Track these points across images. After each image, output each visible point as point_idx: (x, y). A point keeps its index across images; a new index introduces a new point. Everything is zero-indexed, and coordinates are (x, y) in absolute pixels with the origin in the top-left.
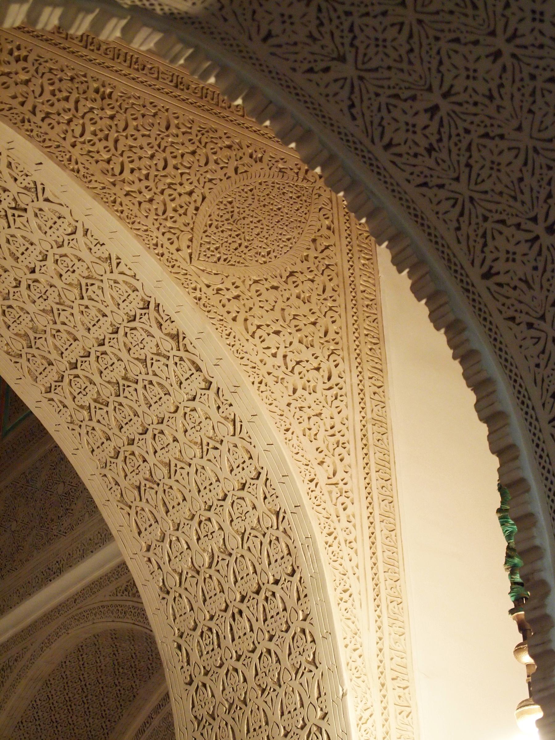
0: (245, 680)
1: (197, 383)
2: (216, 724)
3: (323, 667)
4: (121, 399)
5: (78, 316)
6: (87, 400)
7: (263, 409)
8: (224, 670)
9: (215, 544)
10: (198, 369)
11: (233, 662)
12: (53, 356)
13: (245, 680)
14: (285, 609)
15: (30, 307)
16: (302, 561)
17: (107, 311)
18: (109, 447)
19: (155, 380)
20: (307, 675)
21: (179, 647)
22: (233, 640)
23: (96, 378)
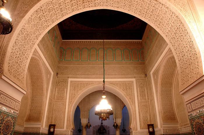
1: (161, 4)
3: (189, 33)
4: (153, 13)
5: (144, 5)
6: (149, 16)
7: (170, 4)
9: (170, 26)
10: (161, 3)
12: (144, 12)
15: (139, 7)
16: (182, 21)
17: (147, 2)
18: (154, 21)
19: (156, 8)
20: (187, 35)
23: (149, 12)
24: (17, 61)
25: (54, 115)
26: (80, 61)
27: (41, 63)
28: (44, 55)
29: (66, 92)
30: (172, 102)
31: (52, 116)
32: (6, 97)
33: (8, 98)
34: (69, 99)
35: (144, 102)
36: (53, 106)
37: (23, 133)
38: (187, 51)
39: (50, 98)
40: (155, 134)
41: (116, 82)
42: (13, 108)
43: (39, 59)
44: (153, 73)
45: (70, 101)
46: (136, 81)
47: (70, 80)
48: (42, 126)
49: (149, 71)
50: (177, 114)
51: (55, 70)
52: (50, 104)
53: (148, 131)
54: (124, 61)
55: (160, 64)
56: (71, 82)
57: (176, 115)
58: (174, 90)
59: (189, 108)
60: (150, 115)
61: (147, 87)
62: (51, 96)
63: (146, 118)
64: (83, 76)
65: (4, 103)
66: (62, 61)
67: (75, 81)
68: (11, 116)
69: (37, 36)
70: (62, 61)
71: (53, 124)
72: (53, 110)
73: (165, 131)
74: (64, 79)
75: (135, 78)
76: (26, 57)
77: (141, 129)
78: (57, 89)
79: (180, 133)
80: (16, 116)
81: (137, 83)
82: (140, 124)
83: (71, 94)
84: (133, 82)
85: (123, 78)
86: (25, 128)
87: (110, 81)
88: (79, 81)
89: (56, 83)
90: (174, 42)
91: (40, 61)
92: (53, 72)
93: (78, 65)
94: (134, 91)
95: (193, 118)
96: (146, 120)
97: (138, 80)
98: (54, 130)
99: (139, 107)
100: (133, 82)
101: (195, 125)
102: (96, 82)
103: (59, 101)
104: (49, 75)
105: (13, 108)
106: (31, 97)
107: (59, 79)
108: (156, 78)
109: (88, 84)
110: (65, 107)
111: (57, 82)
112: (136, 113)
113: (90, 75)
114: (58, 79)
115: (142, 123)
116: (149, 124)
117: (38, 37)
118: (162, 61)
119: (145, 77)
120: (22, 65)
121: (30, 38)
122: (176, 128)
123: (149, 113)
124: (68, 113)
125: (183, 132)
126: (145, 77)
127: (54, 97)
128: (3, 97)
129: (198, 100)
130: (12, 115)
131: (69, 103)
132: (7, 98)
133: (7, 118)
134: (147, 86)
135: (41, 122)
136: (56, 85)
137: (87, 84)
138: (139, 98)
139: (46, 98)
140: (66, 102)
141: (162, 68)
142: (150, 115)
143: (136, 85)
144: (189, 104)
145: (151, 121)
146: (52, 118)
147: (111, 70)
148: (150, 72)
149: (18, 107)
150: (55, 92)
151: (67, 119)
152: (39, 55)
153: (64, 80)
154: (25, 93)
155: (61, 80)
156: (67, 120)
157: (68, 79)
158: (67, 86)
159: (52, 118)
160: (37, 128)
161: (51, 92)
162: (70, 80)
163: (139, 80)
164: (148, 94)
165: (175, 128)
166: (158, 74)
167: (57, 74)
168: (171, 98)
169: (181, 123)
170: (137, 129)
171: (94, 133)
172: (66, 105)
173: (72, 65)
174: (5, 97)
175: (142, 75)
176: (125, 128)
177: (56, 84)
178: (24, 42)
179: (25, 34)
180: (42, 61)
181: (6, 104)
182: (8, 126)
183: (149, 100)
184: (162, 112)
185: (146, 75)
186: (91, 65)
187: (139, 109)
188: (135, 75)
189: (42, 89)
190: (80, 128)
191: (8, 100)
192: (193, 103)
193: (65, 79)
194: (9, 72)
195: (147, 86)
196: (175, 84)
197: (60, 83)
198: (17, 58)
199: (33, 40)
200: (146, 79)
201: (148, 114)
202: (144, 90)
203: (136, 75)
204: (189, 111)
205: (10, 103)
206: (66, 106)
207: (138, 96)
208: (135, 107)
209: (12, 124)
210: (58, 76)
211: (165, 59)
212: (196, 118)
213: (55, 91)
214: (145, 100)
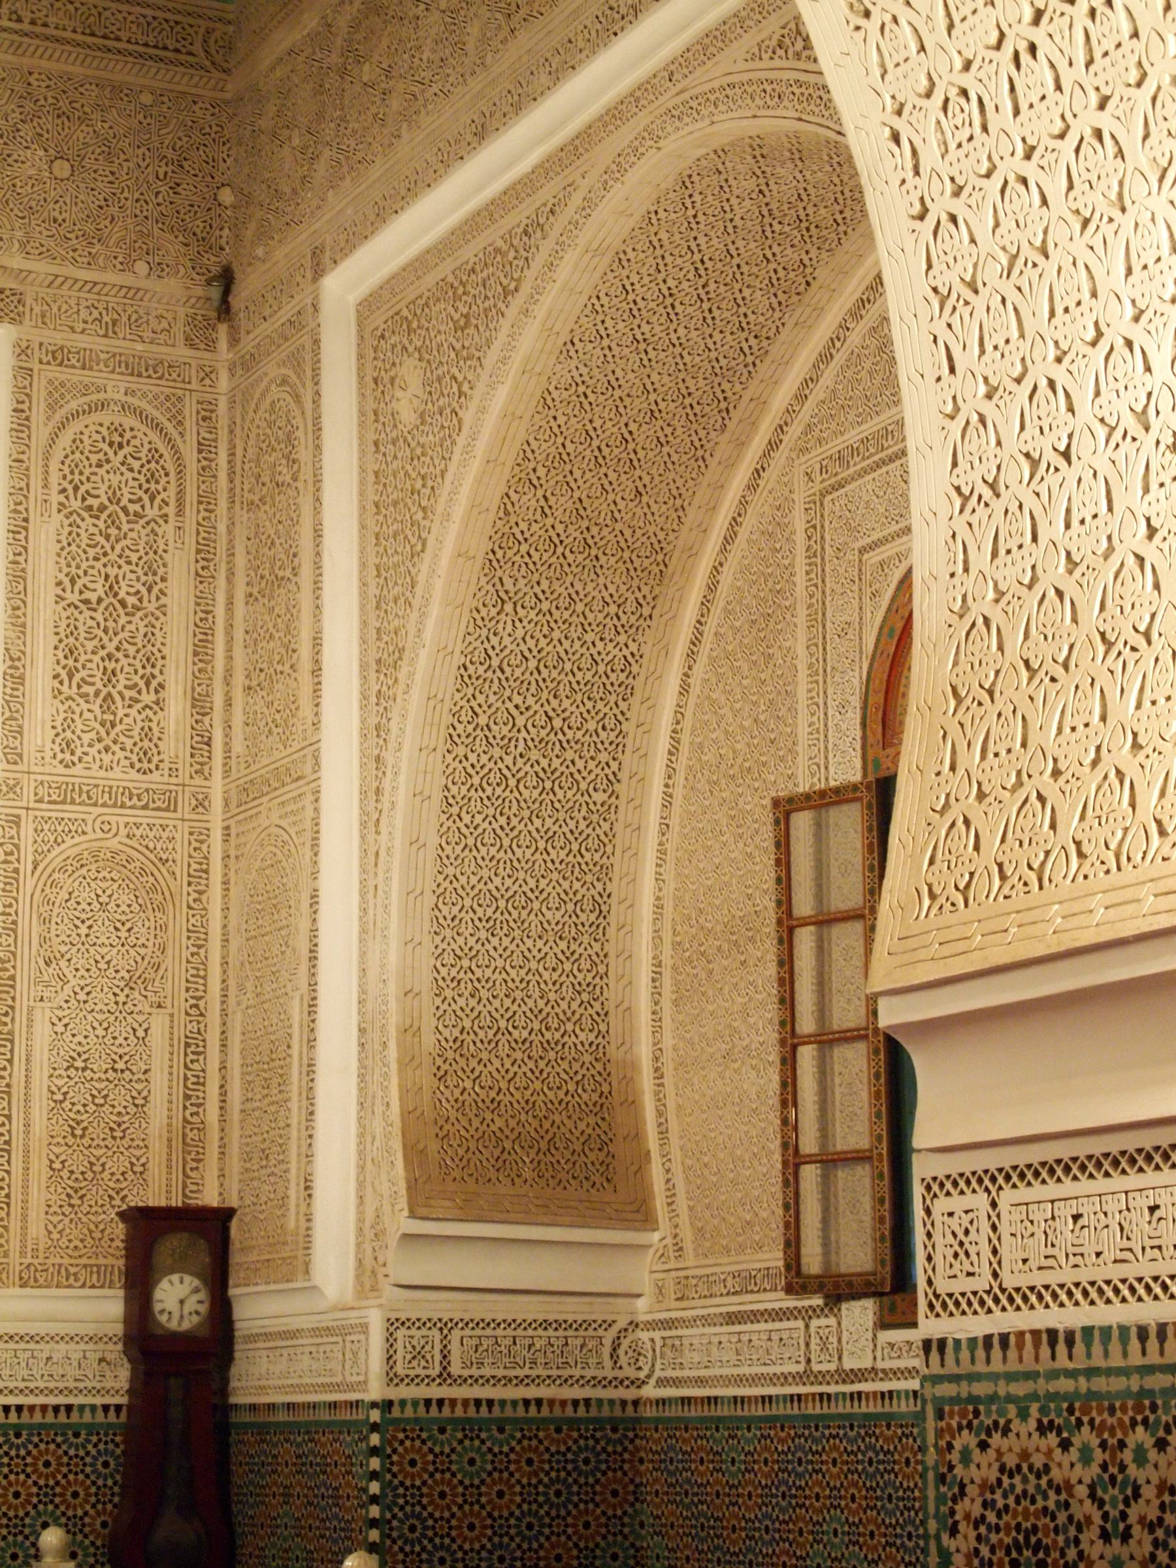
0: (1044, 202)
2: (978, 302)
8: (997, 181)
11: (1017, 165)
13: (1044, 202)
14: (1135, 35)
21: (896, 138)
22: (1017, 112)
30: (605, 872)
35: (119, 799)
38: (1120, 408)
40: (234, 1371)
44: (367, 307)
49: (298, 243)
50: (646, 1081)
53: (119, 1329)
55: (546, 194)
57: (633, 1104)
58: (684, 689)
59: (961, 1251)
60: (193, 1046)
61: (206, 531)
63: (120, 1098)
73: (418, 1355)
79: (650, 1391)
81: (40, 432)
90: (969, 167)
95: (973, 1399)
96: (117, 1131)
97: (59, 356)
101: (985, 1486)
108: (408, 416)
116: (157, 1198)
118: (603, 154)
122: (598, 1310)
123: (181, 1002)
125: (701, 1381)
129: (1101, 1184)
134: (206, 501)
141: (563, 272)
142: (193, 1046)
144: (969, 1201)
148: (318, 273)
163: (76, 376)
164: (201, 651)
165: (572, 1310)
166: (471, 357)
168: (609, 808)
169: (687, 1234)
175: (158, 269)
184: (429, 1023)
185: (227, 279)
188: (16, 262)
192: (1024, 1193)
195: (206, 501)
196: (726, 579)
200: (208, 374)
201: (159, 1025)
203: (42, 267)
204: (943, 1286)
211: (652, 136)
212: (1024, 1415)
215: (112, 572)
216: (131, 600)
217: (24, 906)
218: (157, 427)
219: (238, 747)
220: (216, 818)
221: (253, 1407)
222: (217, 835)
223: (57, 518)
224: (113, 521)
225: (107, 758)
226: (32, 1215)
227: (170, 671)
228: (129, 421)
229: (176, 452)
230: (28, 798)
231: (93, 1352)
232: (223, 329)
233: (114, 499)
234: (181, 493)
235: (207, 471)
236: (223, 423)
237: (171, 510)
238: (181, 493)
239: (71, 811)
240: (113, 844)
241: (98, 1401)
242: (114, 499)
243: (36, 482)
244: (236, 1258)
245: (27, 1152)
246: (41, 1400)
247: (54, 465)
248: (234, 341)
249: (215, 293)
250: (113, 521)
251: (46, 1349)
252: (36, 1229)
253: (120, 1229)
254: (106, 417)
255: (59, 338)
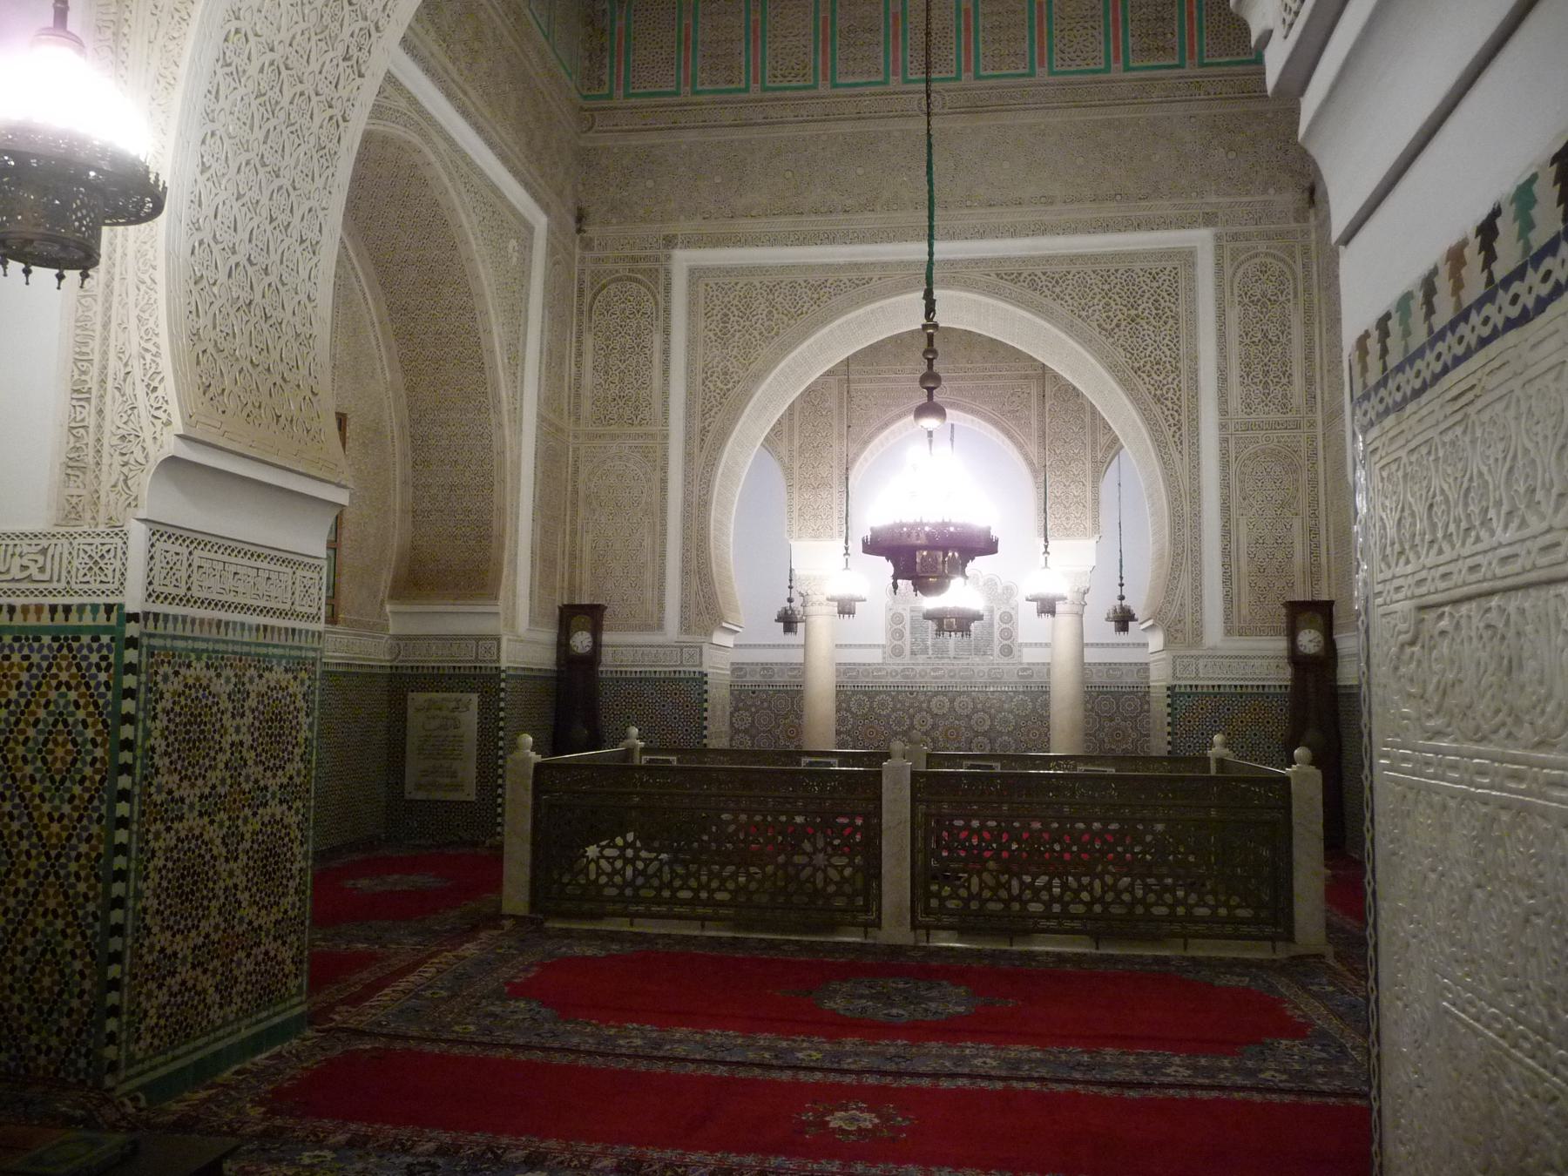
24: (245, 296)
25: (590, 536)
26: (755, 92)
27: (438, 165)
28: (450, 96)
29: (657, 358)
31: (573, 542)
32: (225, 558)
33: (239, 560)
34: (689, 415)
36: (576, 471)
37: (388, 671)
39: (542, 419)
41: (1048, 259)
42: (287, 607)
43: (416, 140)
45: (698, 425)
46: (1219, 247)
47: (683, 259)
48: (512, 624)
51: (560, 194)
52: (549, 458)
53: (1285, 653)
54: (1127, 69)
56: (695, 274)
60: (1313, 531)
62: (549, 402)
63: (1280, 555)
64: (783, 223)
65: (223, 598)
66: (606, 103)
67: (728, 271)
68: (282, 657)
69: (353, 51)
70: (606, 103)
71: (586, 601)
72: (575, 504)
74: (634, 259)
75: (1209, 220)
76: (302, 241)
77: (1229, 632)
78: (589, 341)
80: (311, 654)
81: (1228, 271)
82: (1228, 598)
83: (699, 379)
84: (1188, 257)
85: (1105, 227)
86: (397, 637)
87: (1001, 261)
88: (752, 270)
89: (581, 292)
91: (426, 150)
92: (546, 208)
93: (739, 135)
94: (1193, 336)
97: (1235, 237)
98: (597, 644)
99: (1225, 464)
100: (1188, 257)
102: (885, 265)
103: (614, 429)
104: (513, 243)
105: (281, 606)
106: (402, 427)
107: (599, 260)
109: (823, 285)
110: (658, 475)
111: (587, 284)
112: (1197, 515)
113: (842, 217)
114: (588, 254)
115: (1245, 588)
116: (1299, 596)
117: (363, 55)
119: (1301, 216)
120: (289, 310)
121: (299, 88)
124: (687, 517)
126: (1301, 216)
127: (578, 406)
128: (206, 565)
130: (287, 652)
131: (688, 439)
132: (233, 559)
133: (261, 676)
134: (1307, 290)
135: (502, 594)
136: (581, 312)
137: (816, 288)
138: (1235, 390)
139: (517, 420)
140: (666, 437)
142: (1313, 531)
143: (1219, 287)
145: (1313, 573)
146: (573, 556)
147: (1006, 165)
149: (314, 591)
150: (579, 365)
151: (685, 560)
152: (413, 101)
153: (643, 265)
154: (342, 497)
155: (609, 266)
156: (685, 572)
157: (669, 257)
158: (667, 311)
159: (573, 556)
160: (478, 638)
161: (549, 365)
162: (683, 259)
163: (1242, 245)
164: (1309, 357)
167: (581, 218)
170: (1198, 634)
171: (902, 636)
172: (665, 457)
173: (691, 136)
174: (219, 556)
176: (1124, 603)
177: (580, 305)
178: (261, 135)
179: (252, 70)
180: (442, 146)
181: (236, 600)
182: (278, 717)
183: (1312, 410)
185: (1312, 191)
186: (846, 127)
187: (1225, 485)
188: (1214, 199)
189: (477, 362)
190: (790, 600)
191: (239, 570)
193: (646, 258)
194: (208, 395)
195: (1307, 290)
197: (613, 286)
198: (238, 275)
199: (327, 91)
200: (1306, 233)
201: (1297, 523)
202: (1285, 328)
205: (263, 586)
206: (664, 469)
207: (1223, 378)
208: (1196, 466)
209: (300, 703)
210: (592, 231)
213: (580, 354)
214: (1284, 407)
215: (1265, 328)
216: (1274, 339)
217: (1232, 476)
218: (1283, 260)
219: (1326, 395)
220: (1319, 430)
221: (1345, 687)
222: (1320, 438)
223: (1238, 308)
224: (1264, 305)
225: (1266, 409)
226: (1243, 606)
227: (1295, 367)
228: (1269, 260)
229: (1293, 272)
230: (1231, 429)
231: (1273, 663)
232: (1312, 211)
233: (1264, 295)
234: (1295, 288)
235: (1308, 277)
236: (1314, 255)
237: (1291, 297)
238: (1295, 288)
239: (1250, 434)
240: (1271, 446)
241: (1277, 683)
242: (1264, 295)
243: (1228, 294)
244: (1336, 622)
245: (1239, 580)
246: (1251, 683)
247: (1235, 285)
248: (1316, 216)
249: (1306, 195)
250: (1264, 305)
251: (1252, 662)
252: (1245, 612)
253: (1284, 611)
254: (1257, 260)
255: (1234, 229)
